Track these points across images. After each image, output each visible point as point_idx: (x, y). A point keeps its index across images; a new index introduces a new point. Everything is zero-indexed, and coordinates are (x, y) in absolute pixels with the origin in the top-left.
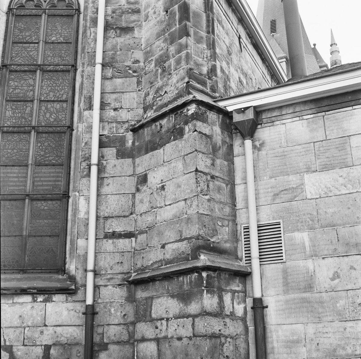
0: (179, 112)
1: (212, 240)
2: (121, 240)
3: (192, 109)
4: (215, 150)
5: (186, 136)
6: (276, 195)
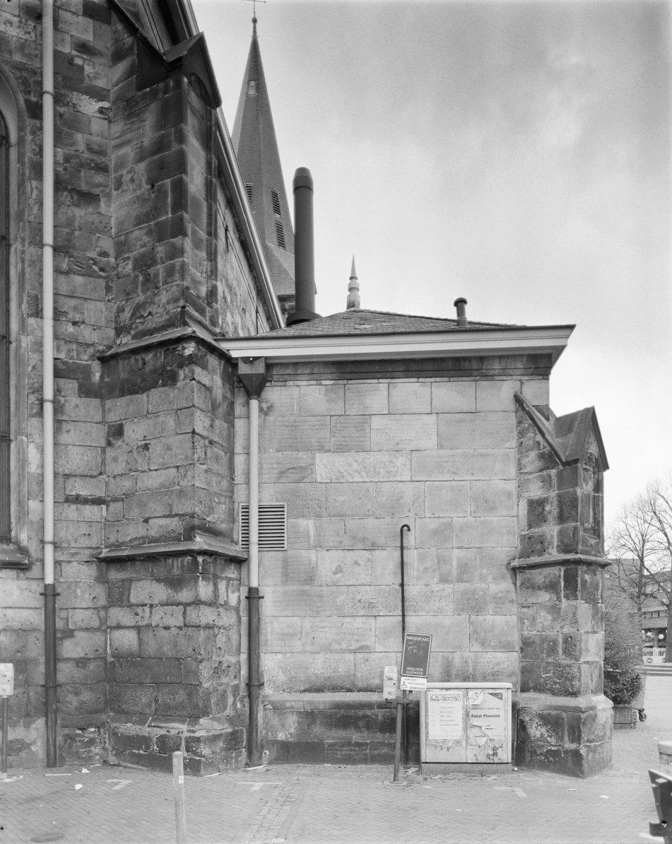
0: (171, 348)
1: (208, 519)
2: (87, 507)
3: (190, 349)
4: (214, 407)
5: (180, 384)
6: (282, 473)
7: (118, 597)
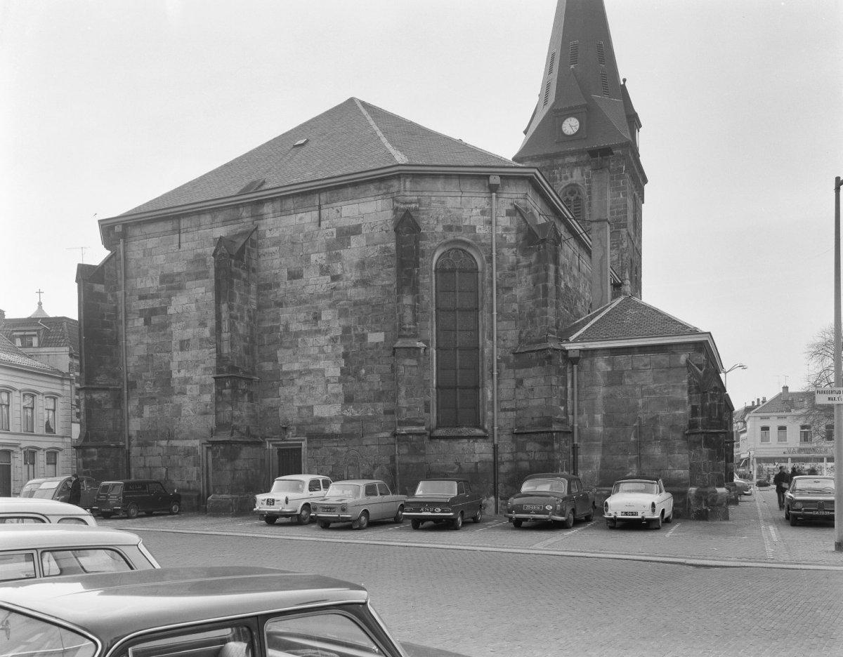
7: (521, 448)
